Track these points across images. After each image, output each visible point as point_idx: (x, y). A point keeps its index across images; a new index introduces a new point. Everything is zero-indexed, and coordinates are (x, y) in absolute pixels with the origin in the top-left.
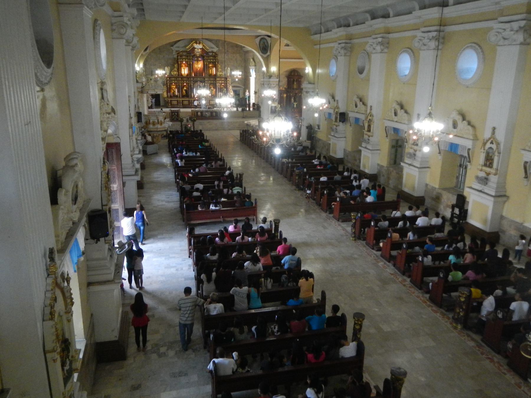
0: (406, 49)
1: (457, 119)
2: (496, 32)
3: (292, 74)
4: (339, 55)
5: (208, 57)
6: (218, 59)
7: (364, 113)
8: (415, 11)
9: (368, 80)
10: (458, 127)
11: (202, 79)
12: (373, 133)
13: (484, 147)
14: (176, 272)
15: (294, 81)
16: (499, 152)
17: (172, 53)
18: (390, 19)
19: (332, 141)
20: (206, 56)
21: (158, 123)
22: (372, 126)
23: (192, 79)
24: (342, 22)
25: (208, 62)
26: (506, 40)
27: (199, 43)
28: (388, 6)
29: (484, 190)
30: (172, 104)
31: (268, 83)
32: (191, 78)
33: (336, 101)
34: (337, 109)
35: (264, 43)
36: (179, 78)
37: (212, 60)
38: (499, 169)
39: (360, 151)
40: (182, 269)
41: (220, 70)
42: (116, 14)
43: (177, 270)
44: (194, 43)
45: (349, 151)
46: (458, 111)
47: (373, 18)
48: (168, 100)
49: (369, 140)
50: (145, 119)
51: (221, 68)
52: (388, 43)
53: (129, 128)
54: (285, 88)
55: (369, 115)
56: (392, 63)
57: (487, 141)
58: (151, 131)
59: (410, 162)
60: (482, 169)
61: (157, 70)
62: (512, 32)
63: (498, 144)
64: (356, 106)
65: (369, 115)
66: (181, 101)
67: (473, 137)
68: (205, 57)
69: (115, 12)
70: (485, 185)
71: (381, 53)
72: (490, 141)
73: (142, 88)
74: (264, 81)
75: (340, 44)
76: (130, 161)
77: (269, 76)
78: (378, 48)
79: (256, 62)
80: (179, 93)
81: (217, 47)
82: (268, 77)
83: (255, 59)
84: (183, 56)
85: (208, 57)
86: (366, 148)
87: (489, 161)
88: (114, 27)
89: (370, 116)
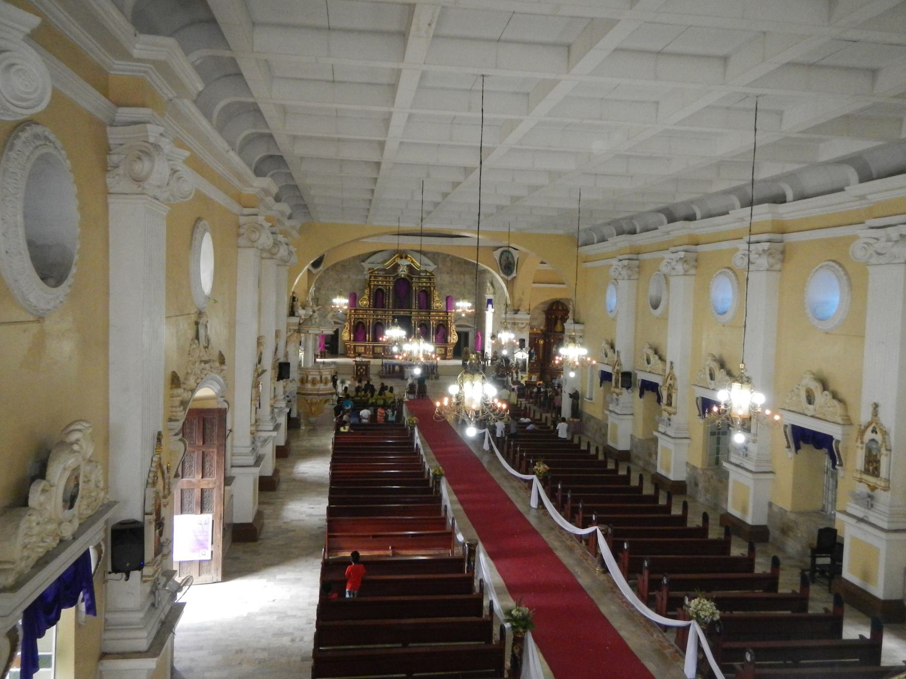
0: (724, 270)
1: (813, 388)
2: (864, 243)
3: (554, 308)
4: (620, 277)
6: (434, 283)
7: (661, 373)
8: (734, 209)
9: (664, 318)
10: (815, 403)
12: (676, 408)
13: (861, 439)
14: (291, 644)
15: (556, 319)
16: (888, 447)
17: (363, 272)
18: (696, 222)
19: (611, 420)
20: (416, 278)
21: (321, 381)
22: (674, 396)
24: (626, 227)
25: (419, 286)
26: (881, 256)
27: (406, 257)
28: (692, 202)
29: (868, 518)
31: (512, 321)
33: (616, 353)
34: (618, 365)
35: (508, 258)
36: (370, 310)
37: (424, 284)
38: (891, 478)
39: (655, 440)
40: (301, 640)
41: (437, 299)
42: (247, 211)
43: (293, 640)
45: (639, 439)
46: (813, 374)
47: (672, 219)
48: (351, 346)
49: (669, 420)
50: (300, 374)
51: (439, 297)
52: (696, 261)
53: (252, 387)
54: (542, 330)
55: (669, 377)
56: (703, 291)
57: (867, 427)
58: (309, 394)
59: (738, 462)
60: (861, 479)
61: (335, 297)
62: (890, 244)
63: (885, 433)
64: (648, 362)
65: (669, 377)
66: (371, 347)
67: (842, 419)
68: (414, 279)
69: (245, 209)
70: (869, 509)
71: (684, 275)
72: (871, 428)
73: (300, 324)
75: (620, 260)
76: (248, 441)
77: (514, 310)
78: (680, 268)
79: (496, 289)
80: (369, 335)
81: (435, 264)
83: (494, 282)
84: (380, 276)
85: (419, 278)
86: (664, 434)
87: (872, 464)
88: (242, 231)
89: (671, 379)
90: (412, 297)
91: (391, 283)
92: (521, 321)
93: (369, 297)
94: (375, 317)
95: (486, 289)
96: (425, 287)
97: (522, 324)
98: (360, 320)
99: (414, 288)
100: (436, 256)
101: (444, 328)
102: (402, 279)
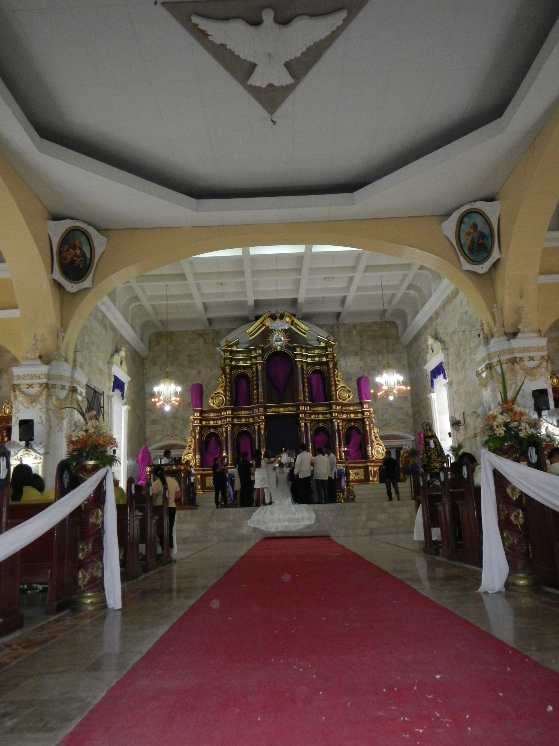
5: (307, 349)
11: (291, 409)
23: (262, 410)
25: (308, 364)
27: (282, 317)
30: (208, 485)
31: (509, 356)
32: (258, 407)
35: (475, 226)
36: (225, 410)
44: (268, 317)
51: (345, 382)
61: (157, 383)
68: (298, 351)
74: (489, 356)
77: (506, 334)
82: (505, 338)
85: (307, 349)
90: (298, 379)
91: (260, 360)
92: (526, 355)
93: (225, 391)
94: (235, 421)
95: (427, 353)
96: (320, 364)
97: (532, 359)
98: (212, 430)
99: (299, 366)
100: (336, 330)
101: (360, 434)
102: (278, 354)
